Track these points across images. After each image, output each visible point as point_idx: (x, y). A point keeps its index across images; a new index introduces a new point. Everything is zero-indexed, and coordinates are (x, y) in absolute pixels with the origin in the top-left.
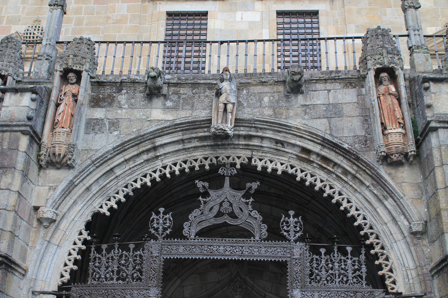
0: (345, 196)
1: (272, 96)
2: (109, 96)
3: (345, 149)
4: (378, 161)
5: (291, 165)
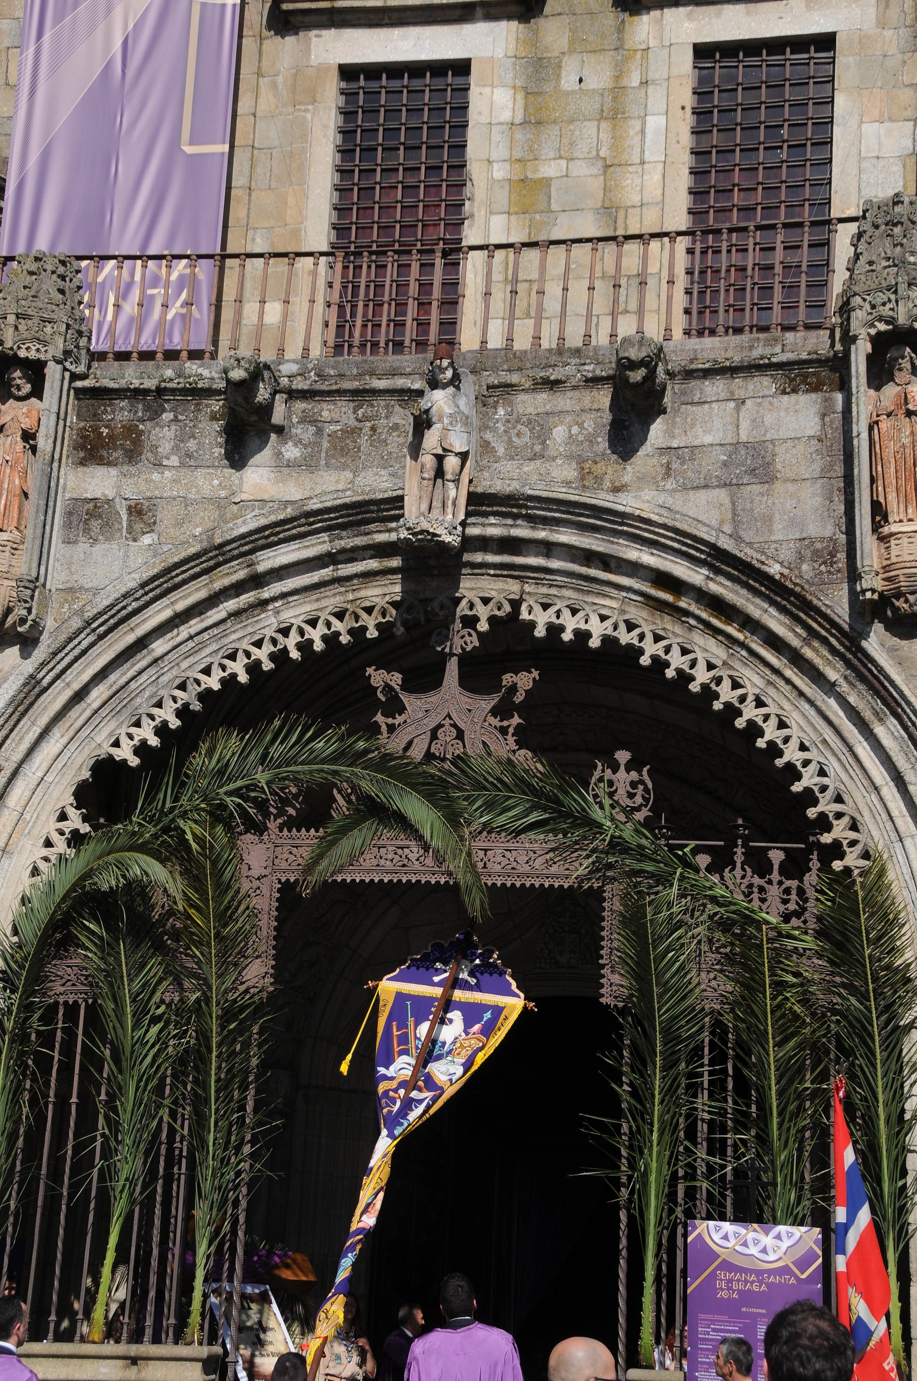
0: (772, 709)
1: (577, 423)
5: (627, 622)
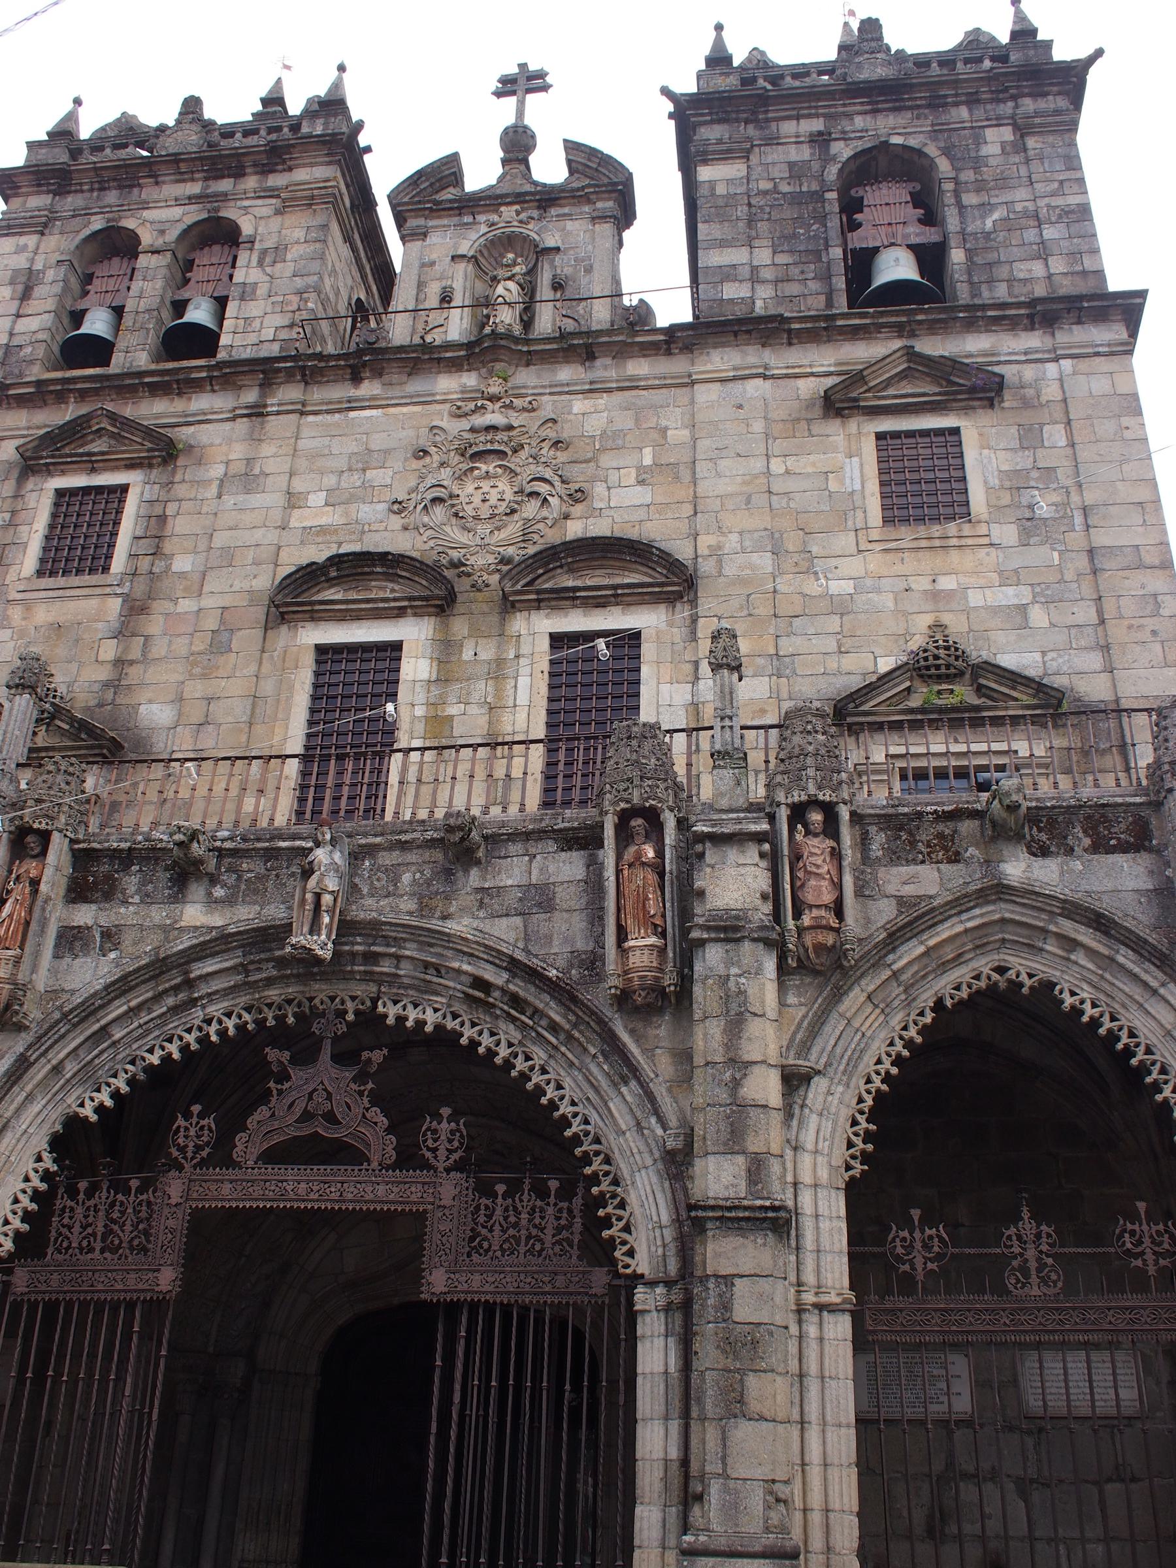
2: (108, 878)
3: (550, 979)
4: (612, 1005)
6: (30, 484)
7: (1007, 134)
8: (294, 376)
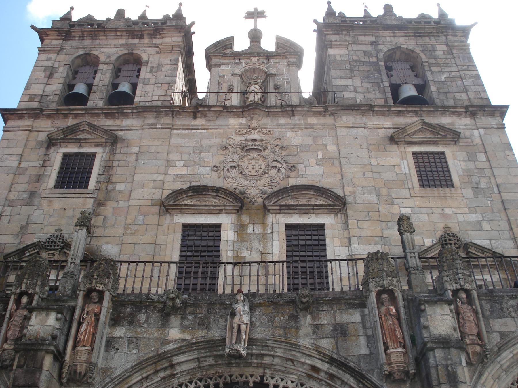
3: (350, 367)
6: (52, 150)
7: (445, 48)
8: (168, 114)
